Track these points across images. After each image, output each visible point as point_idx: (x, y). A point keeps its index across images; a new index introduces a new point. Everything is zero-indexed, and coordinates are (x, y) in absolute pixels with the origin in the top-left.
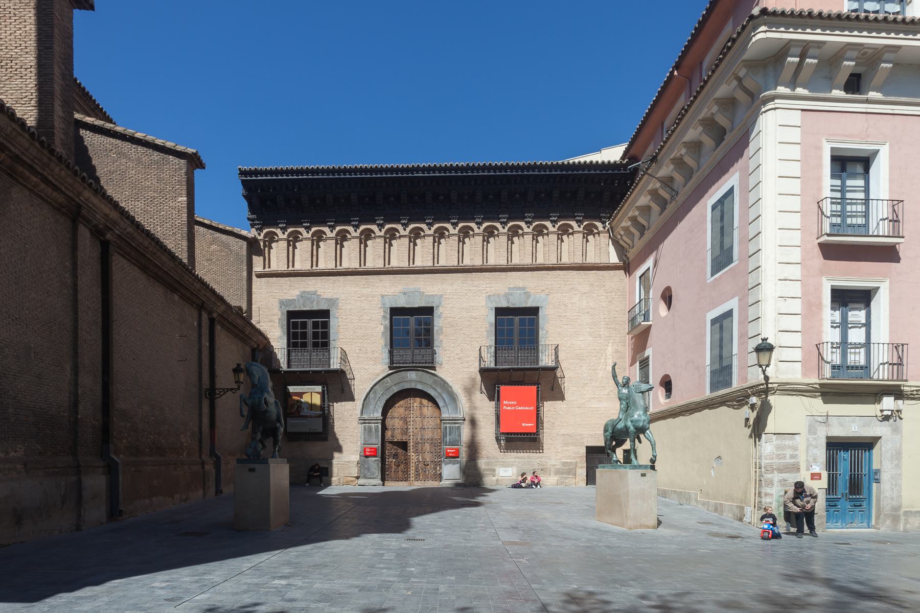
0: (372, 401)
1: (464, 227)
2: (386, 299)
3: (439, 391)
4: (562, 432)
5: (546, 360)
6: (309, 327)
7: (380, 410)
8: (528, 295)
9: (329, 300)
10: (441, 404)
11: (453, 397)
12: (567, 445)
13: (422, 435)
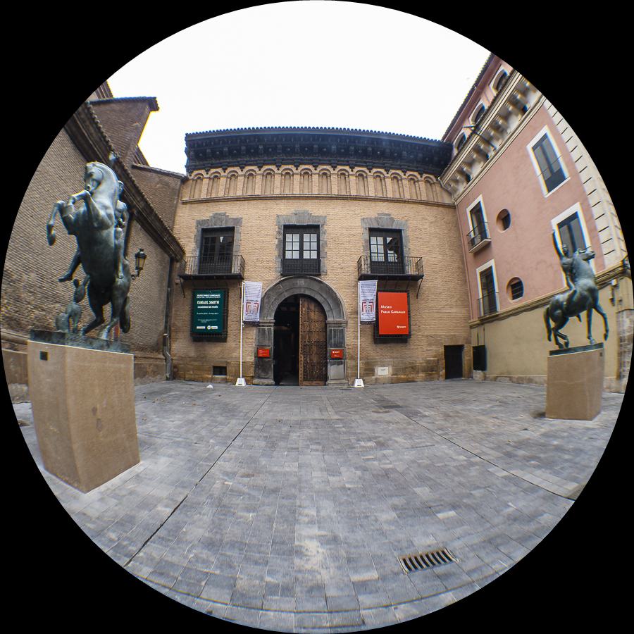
1: (341, 170)
2: (281, 218)
3: (325, 296)
4: (426, 334)
5: (411, 271)
6: (218, 242)
8: (392, 220)
9: (234, 219)
10: (326, 309)
12: (430, 344)
13: (309, 337)
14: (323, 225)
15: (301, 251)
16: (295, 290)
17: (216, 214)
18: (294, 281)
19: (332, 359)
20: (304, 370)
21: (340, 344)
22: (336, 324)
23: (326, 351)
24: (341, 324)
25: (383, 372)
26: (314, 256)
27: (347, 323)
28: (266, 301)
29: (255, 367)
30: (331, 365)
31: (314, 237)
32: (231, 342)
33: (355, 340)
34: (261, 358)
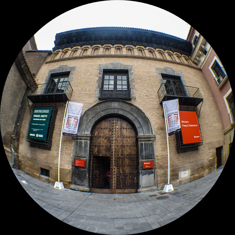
0: (84, 122)
7: (90, 129)
8: (174, 72)
10: (137, 125)
11: (146, 121)
13: (122, 151)
14: (131, 70)
15: (115, 84)
16: (110, 110)
17: (61, 66)
18: (109, 104)
19: (144, 169)
20: (117, 179)
21: (151, 156)
22: (147, 138)
23: (138, 163)
24: (150, 138)
25: (185, 175)
26: (125, 87)
27: (155, 138)
28: (85, 118)
29: (72, 175)
30: (143, 175)
31: (125, 78)
32: (53, 152)
33: (163, 150)
34: (76, 167)
